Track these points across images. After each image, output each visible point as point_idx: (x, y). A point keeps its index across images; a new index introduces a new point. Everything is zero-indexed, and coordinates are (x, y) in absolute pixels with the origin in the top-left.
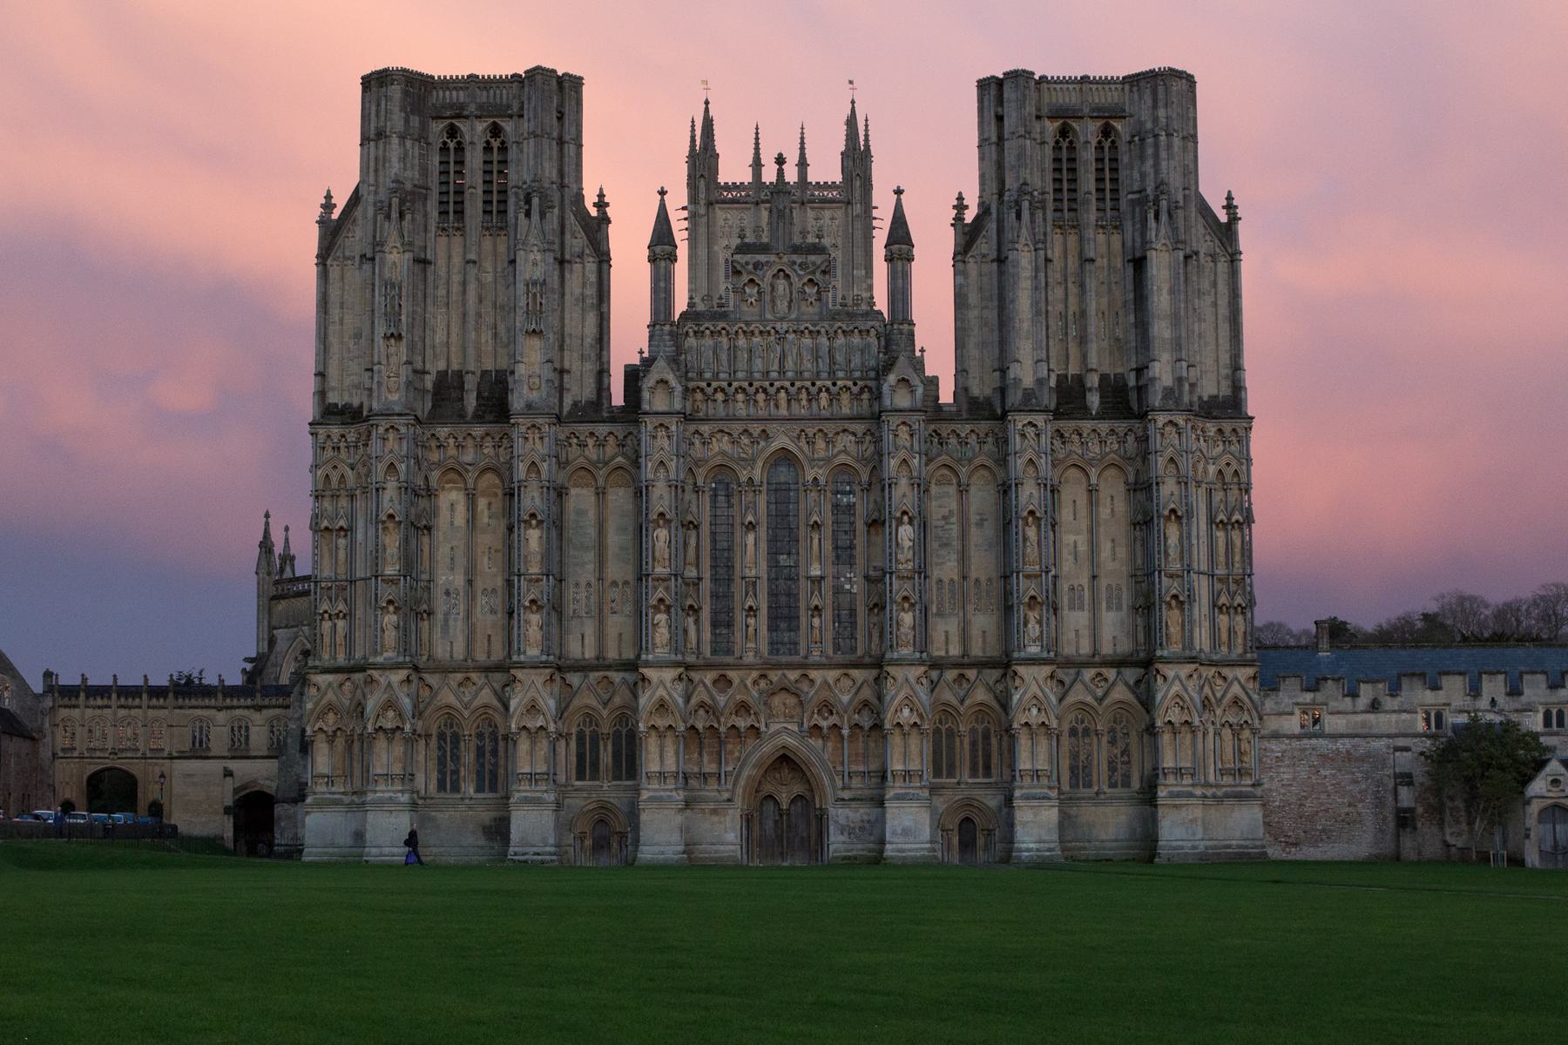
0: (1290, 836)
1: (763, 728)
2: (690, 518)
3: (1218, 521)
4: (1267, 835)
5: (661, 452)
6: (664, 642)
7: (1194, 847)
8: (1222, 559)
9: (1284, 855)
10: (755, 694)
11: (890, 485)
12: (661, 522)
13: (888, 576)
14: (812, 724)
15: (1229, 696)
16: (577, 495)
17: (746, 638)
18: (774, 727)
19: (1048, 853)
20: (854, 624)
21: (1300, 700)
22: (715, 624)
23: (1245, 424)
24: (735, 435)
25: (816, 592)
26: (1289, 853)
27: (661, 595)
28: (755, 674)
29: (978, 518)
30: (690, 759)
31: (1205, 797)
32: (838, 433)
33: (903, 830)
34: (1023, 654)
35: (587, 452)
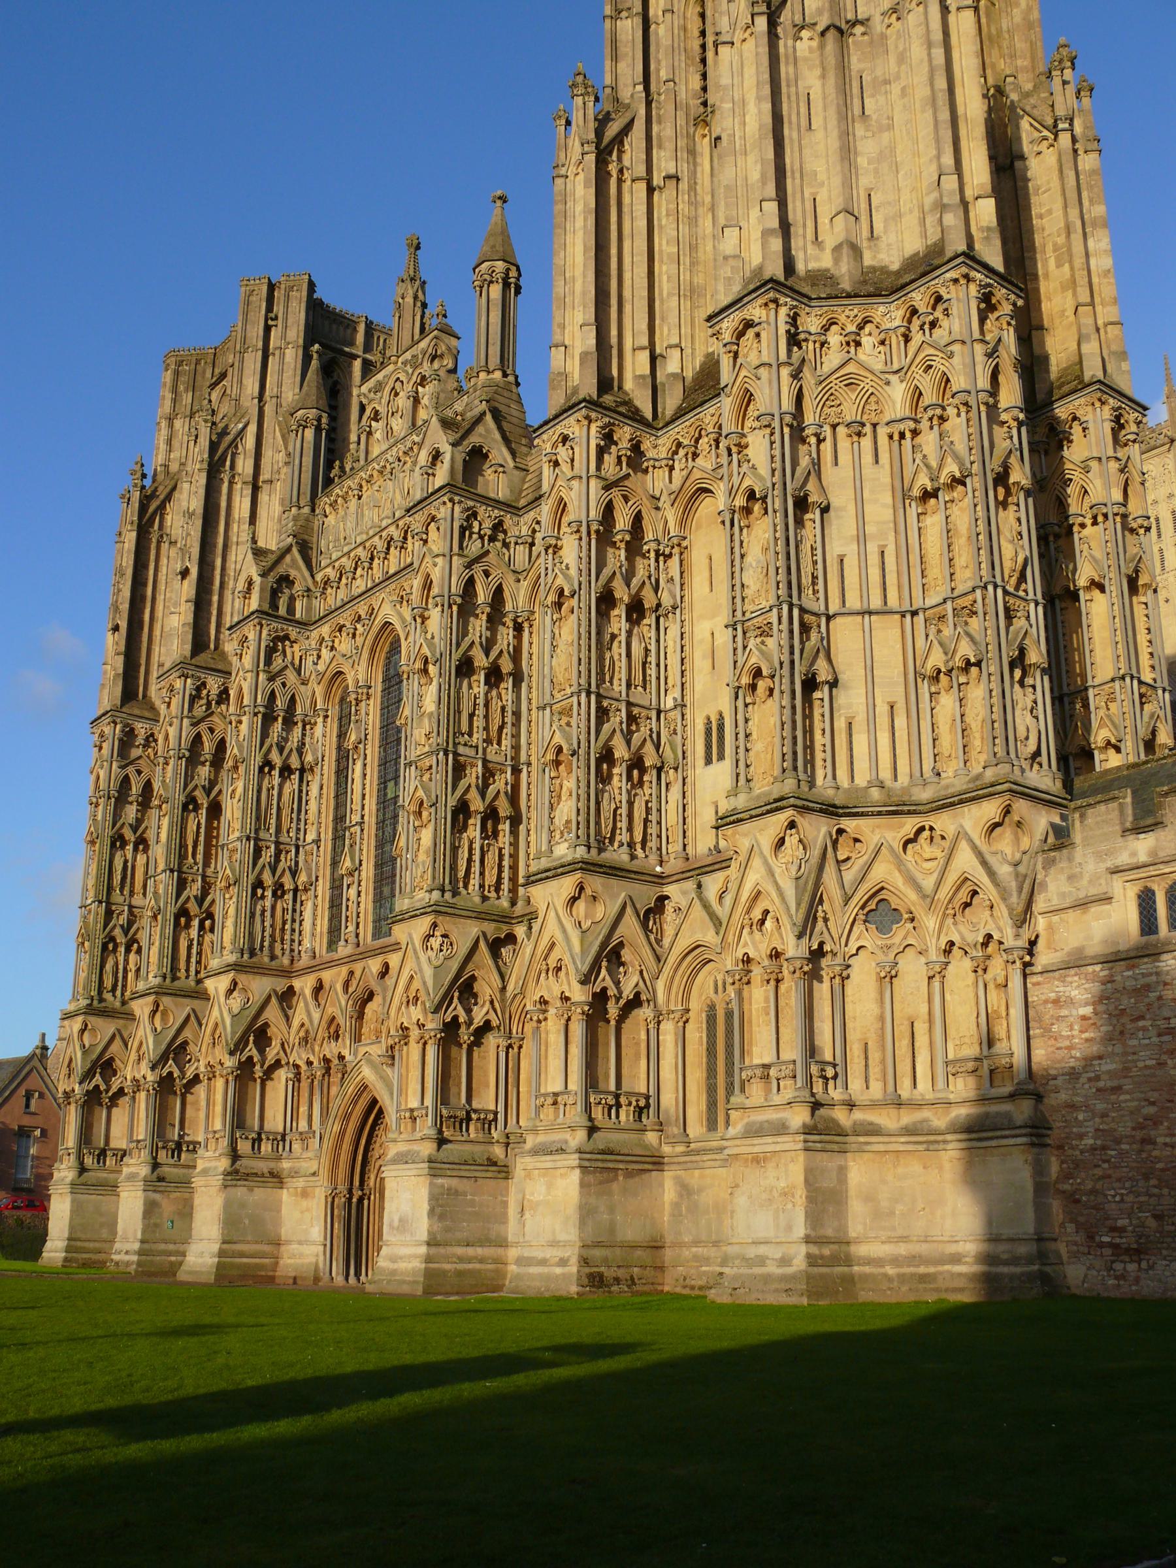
0: (1122, 1230)
1: (348, 1058)
3: (916, 492)
4: (1070, 1228)
7: (785, 1261)
8: (937, 570)
9: (1111, 1282)
10: (343, 1003)
15: (952, 878)
19: (558, 1270)
21: (1124, 859)
23: (948, 275)
24: (348, 625)
26: (1122, 1277)
28: (344, 970)
31: (873, 1130)
33: (401, 1220)
34: (544, 863)
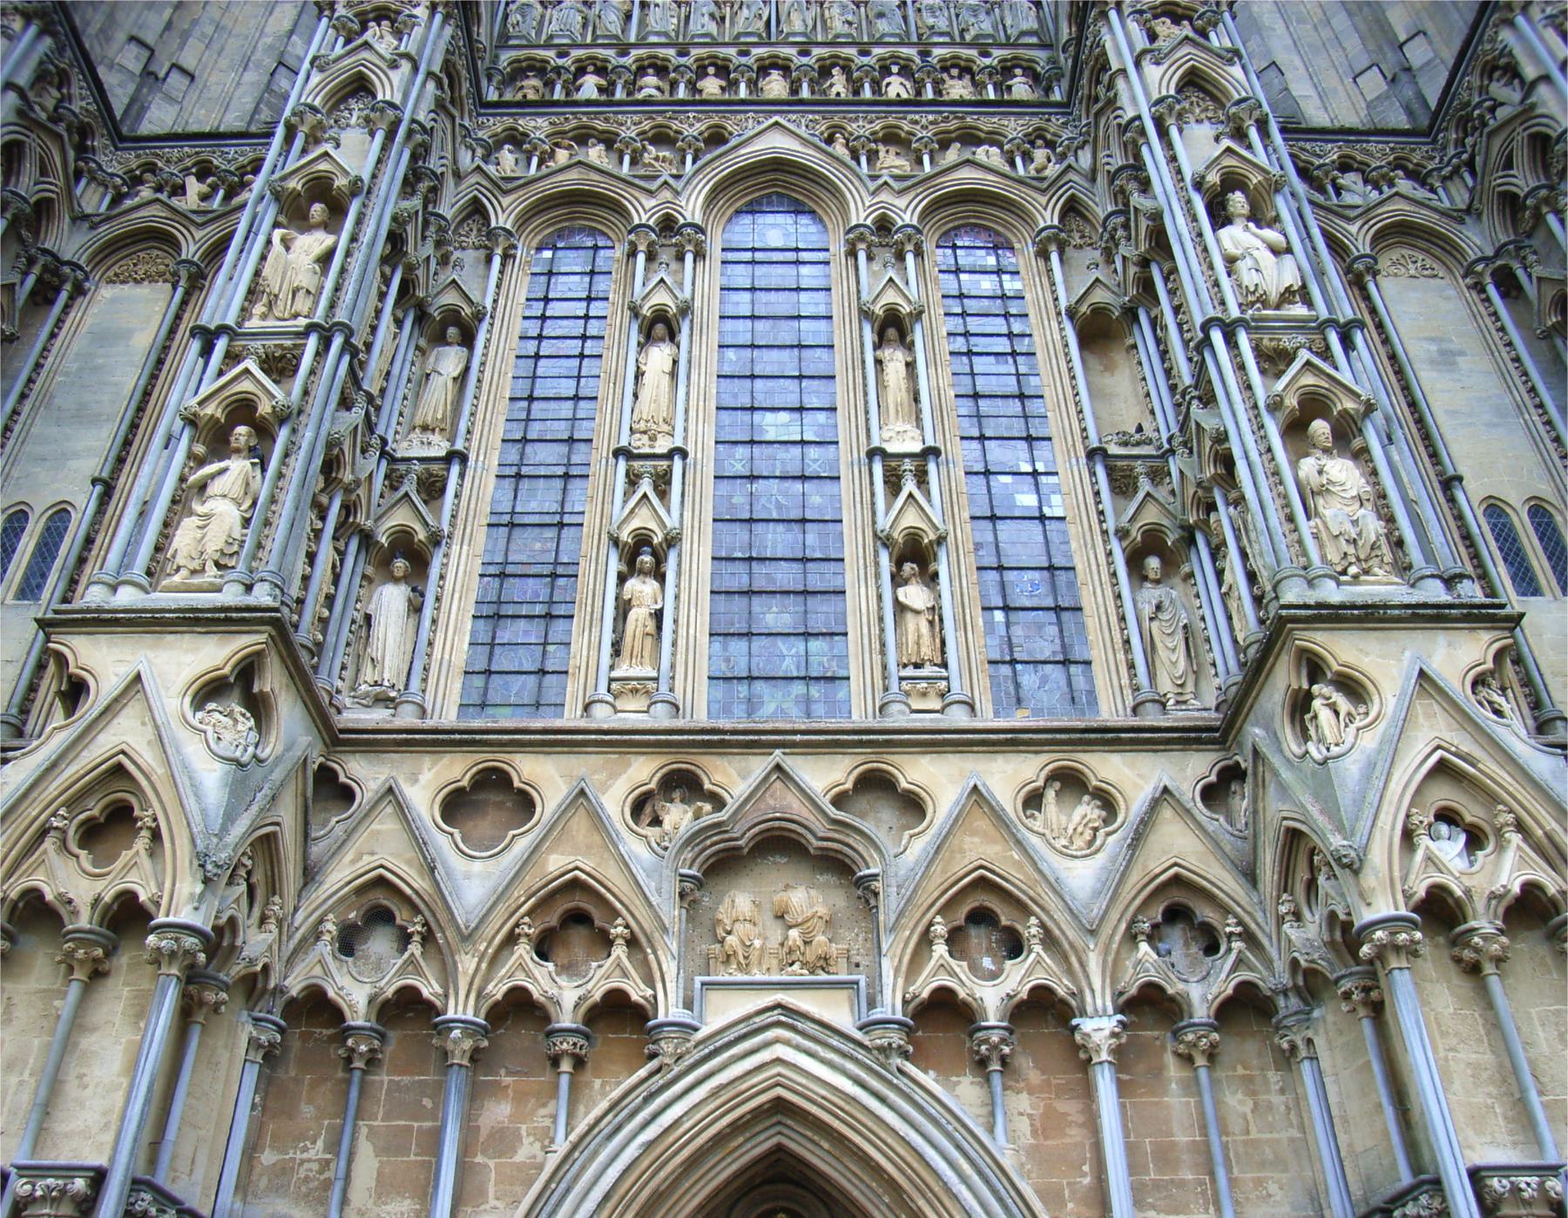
1: (670, 1010)
2: (451, 298)
5: (366, 54)
6: (214, 544)
11: (1159, 123)
12: (317, 210)
13: (1217, 336)
14: (924, 987)
16: (113, 301)
17: (617, 650)
18: (723, 1011)
20: (1064, 611)
22: (493, 614)
25: (909, 486)
27: (246, 385)
28: (644, 771)
29: (1434, 348)
30: (283, 1171)
32: (945, 145)
35: (175, 202)
